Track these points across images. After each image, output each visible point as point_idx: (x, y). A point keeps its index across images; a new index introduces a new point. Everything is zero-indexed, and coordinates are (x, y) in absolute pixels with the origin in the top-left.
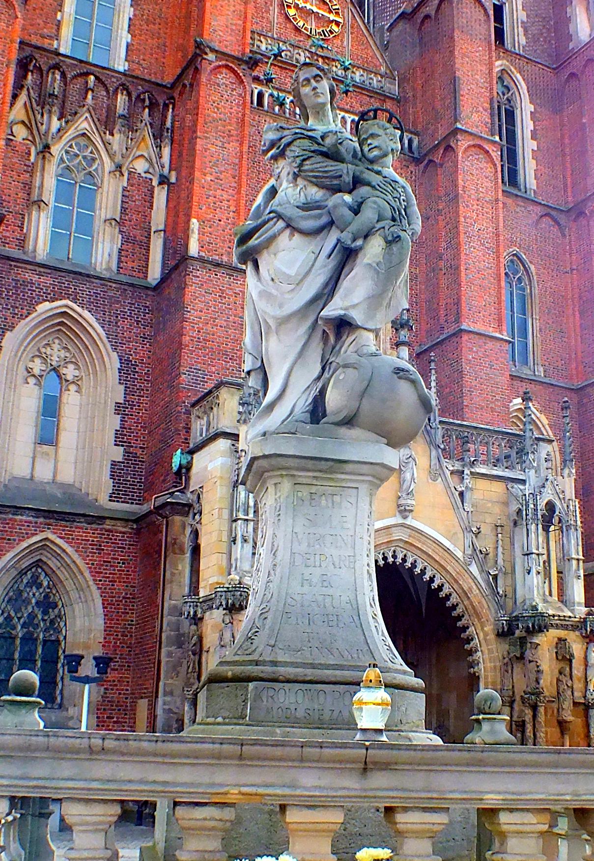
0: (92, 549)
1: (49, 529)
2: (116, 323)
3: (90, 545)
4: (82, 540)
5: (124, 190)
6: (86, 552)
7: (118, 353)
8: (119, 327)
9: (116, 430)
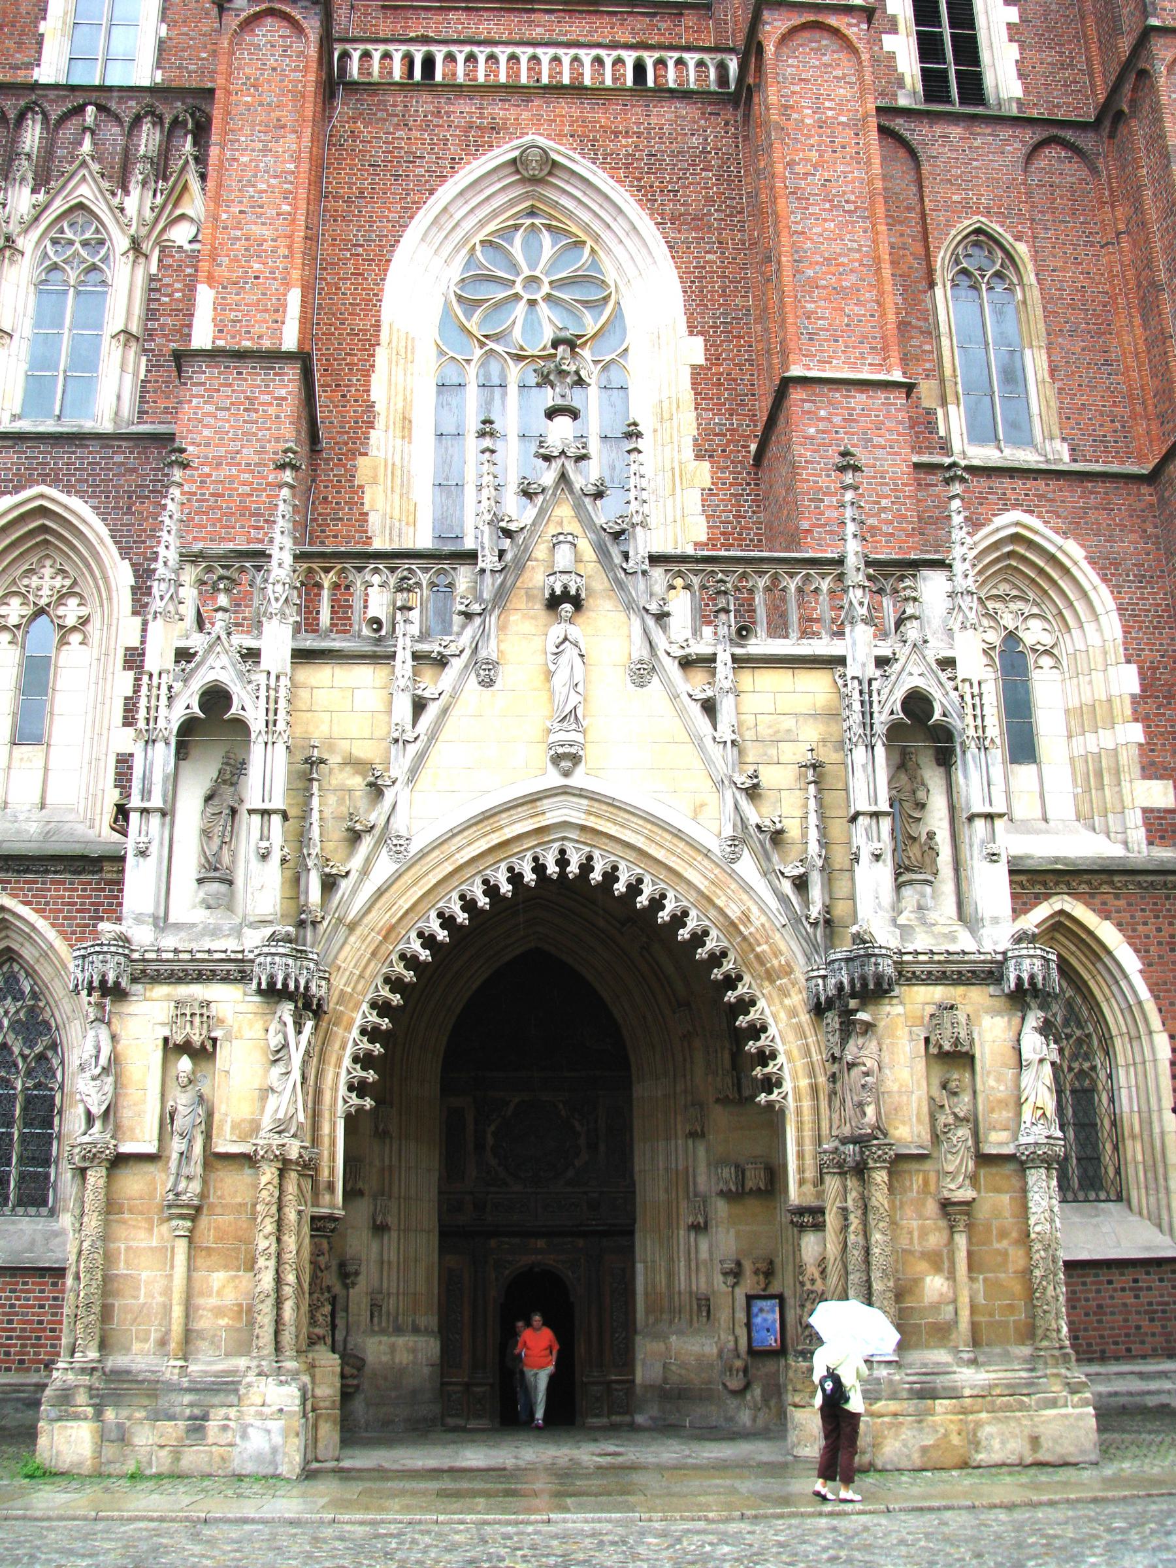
0: (83, 918)
1: (4, 889)
2: (129, 508)
3: (78, 911)
4: (63, 904)
5: (151, 280)
6: (70, 926)
7: (130, 559)
8: (133, 514)
9: (126, 698)
